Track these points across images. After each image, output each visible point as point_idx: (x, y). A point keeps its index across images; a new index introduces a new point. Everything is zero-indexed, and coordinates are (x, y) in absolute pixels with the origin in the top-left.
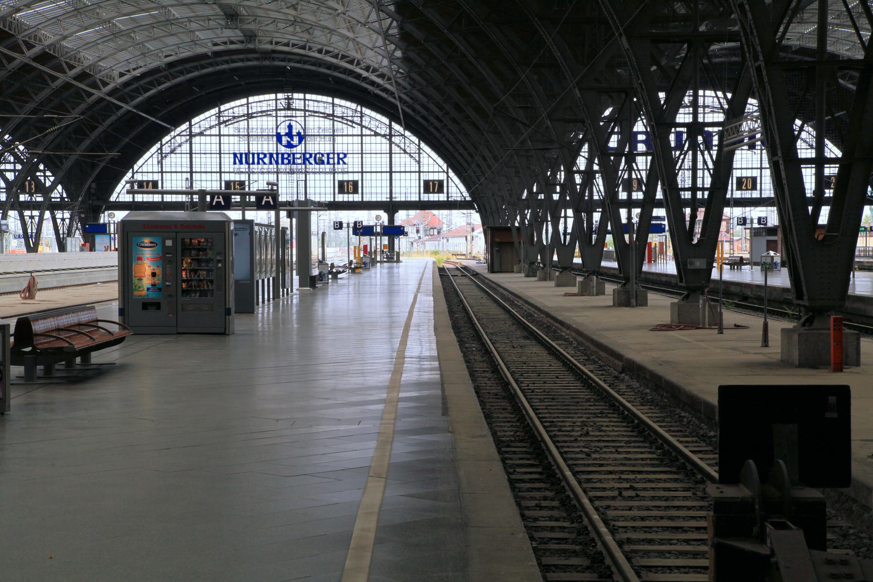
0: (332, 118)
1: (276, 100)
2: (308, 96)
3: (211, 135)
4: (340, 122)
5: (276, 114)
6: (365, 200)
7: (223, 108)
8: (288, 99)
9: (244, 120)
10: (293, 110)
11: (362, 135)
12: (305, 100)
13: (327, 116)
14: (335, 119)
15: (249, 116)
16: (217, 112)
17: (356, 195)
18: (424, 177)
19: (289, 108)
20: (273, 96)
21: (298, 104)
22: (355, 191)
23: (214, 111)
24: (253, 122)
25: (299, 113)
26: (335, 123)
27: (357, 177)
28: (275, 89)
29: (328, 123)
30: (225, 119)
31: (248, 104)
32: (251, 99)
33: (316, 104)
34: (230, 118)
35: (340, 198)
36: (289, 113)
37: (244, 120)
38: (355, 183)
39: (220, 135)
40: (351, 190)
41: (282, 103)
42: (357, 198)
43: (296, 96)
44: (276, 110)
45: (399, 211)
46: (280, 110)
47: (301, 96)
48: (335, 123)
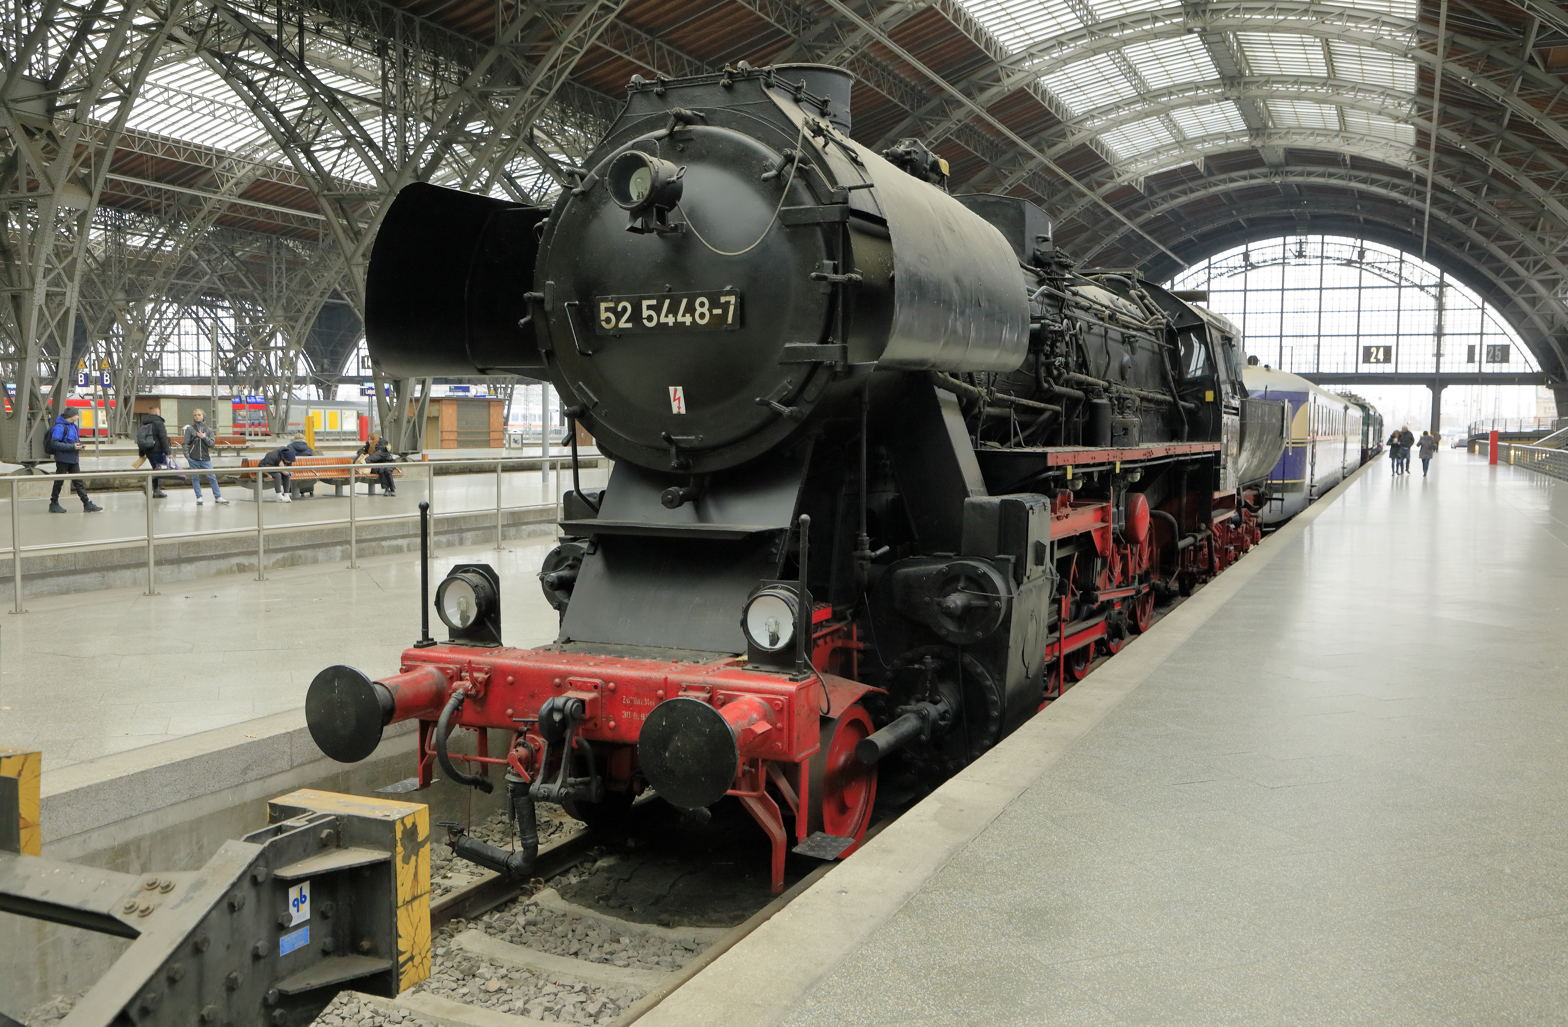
1: (1285, 244)
2: (1328, 238)
6: (1399, 371)
7: (1214, 259)
8: (1301, 243)
11: (1400, 287)
17: (1387, 365)
18: (1489, 340)
20: (1280, 240)
22: (1387, 359)
23: (1204, 263)
24: (1252, 274)
25: (1313, 261)
26: (1363, 272)
27: (1391, 341)
28: (1284, 231)
29: (1353, 272)
30: (1219, 271)
32: (1252, 246)
33: (1338, 247)
35: (1364, 369)
36: (1301, 261)
38: (1387, 350)
40: (1381, 356)
41: (1295, 248)
42: (1389, 368)
43: (1311, 238)
45: (1450, 387)
47: (1318, 238)
48: (1363, 272)
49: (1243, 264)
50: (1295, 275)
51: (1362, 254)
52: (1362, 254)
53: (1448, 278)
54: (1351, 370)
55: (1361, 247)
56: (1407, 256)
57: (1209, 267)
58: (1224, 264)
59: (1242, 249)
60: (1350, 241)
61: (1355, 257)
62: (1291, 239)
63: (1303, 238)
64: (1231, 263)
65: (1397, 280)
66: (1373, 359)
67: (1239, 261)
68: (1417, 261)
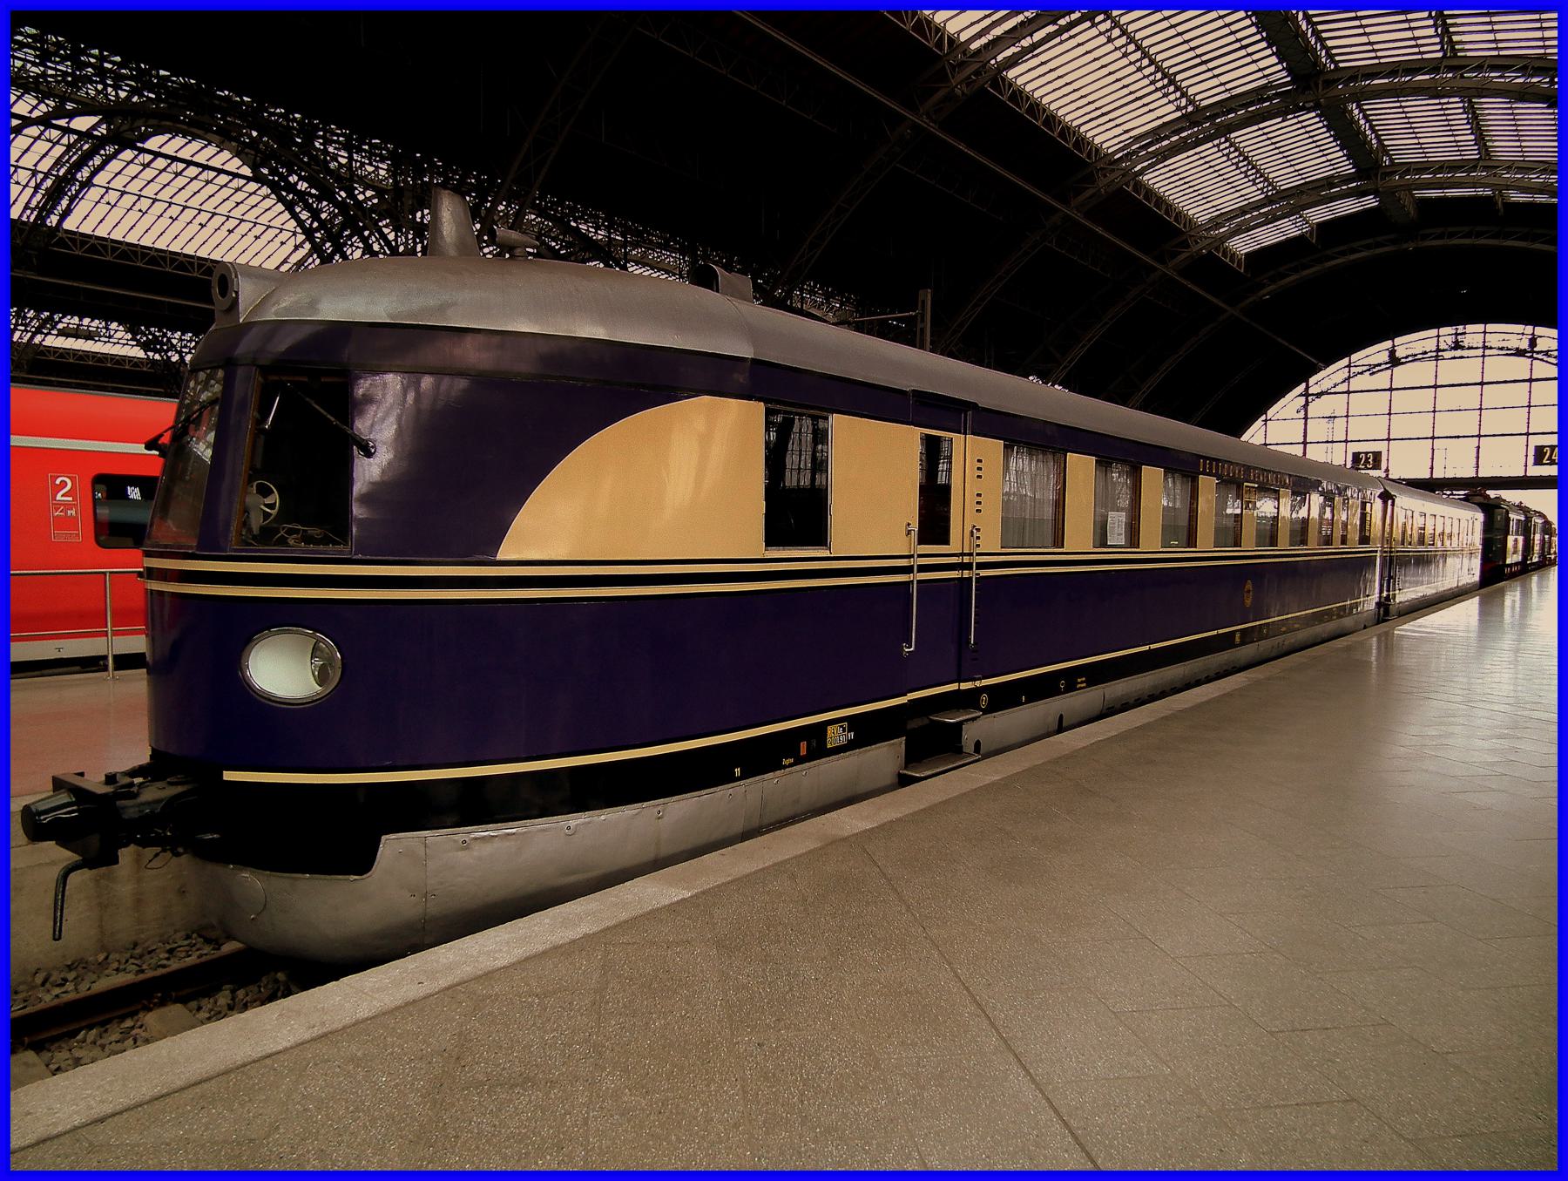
0: (1529, 355)
2: (1491, 327)
3: (1335, 393)
4: (1542, 360)
7: (1354, 357)
10: (1462, 348)
12: (1485, 332)
13: (1519, 353)
14: (1535, 355)
15: (1394, 361)
19: (1457, 346)
20: (1433, 332)
23: (1345, 361)
30: (1360, 369)
31: (1394, 346)
32: (1398, 341)
36: (1459, 353)
41: (1450, 340)
43: (1470, 328)
44: (1438, 350)
46: (1444, 350)
47: (1480, 327)
50: (1451, 370)
51: (1533, 342)
52: (1533, 342)
54: (1517, 471)
55: (1533, 334)
57: (1349, 366)
58: (1366, 362)
59: (1388, 344)
60: (1519, 328)
61: (1524, 345)
62: (1445, 330)
64: (1373, 360)
66: (1544, 461)
67: (1385, 357)
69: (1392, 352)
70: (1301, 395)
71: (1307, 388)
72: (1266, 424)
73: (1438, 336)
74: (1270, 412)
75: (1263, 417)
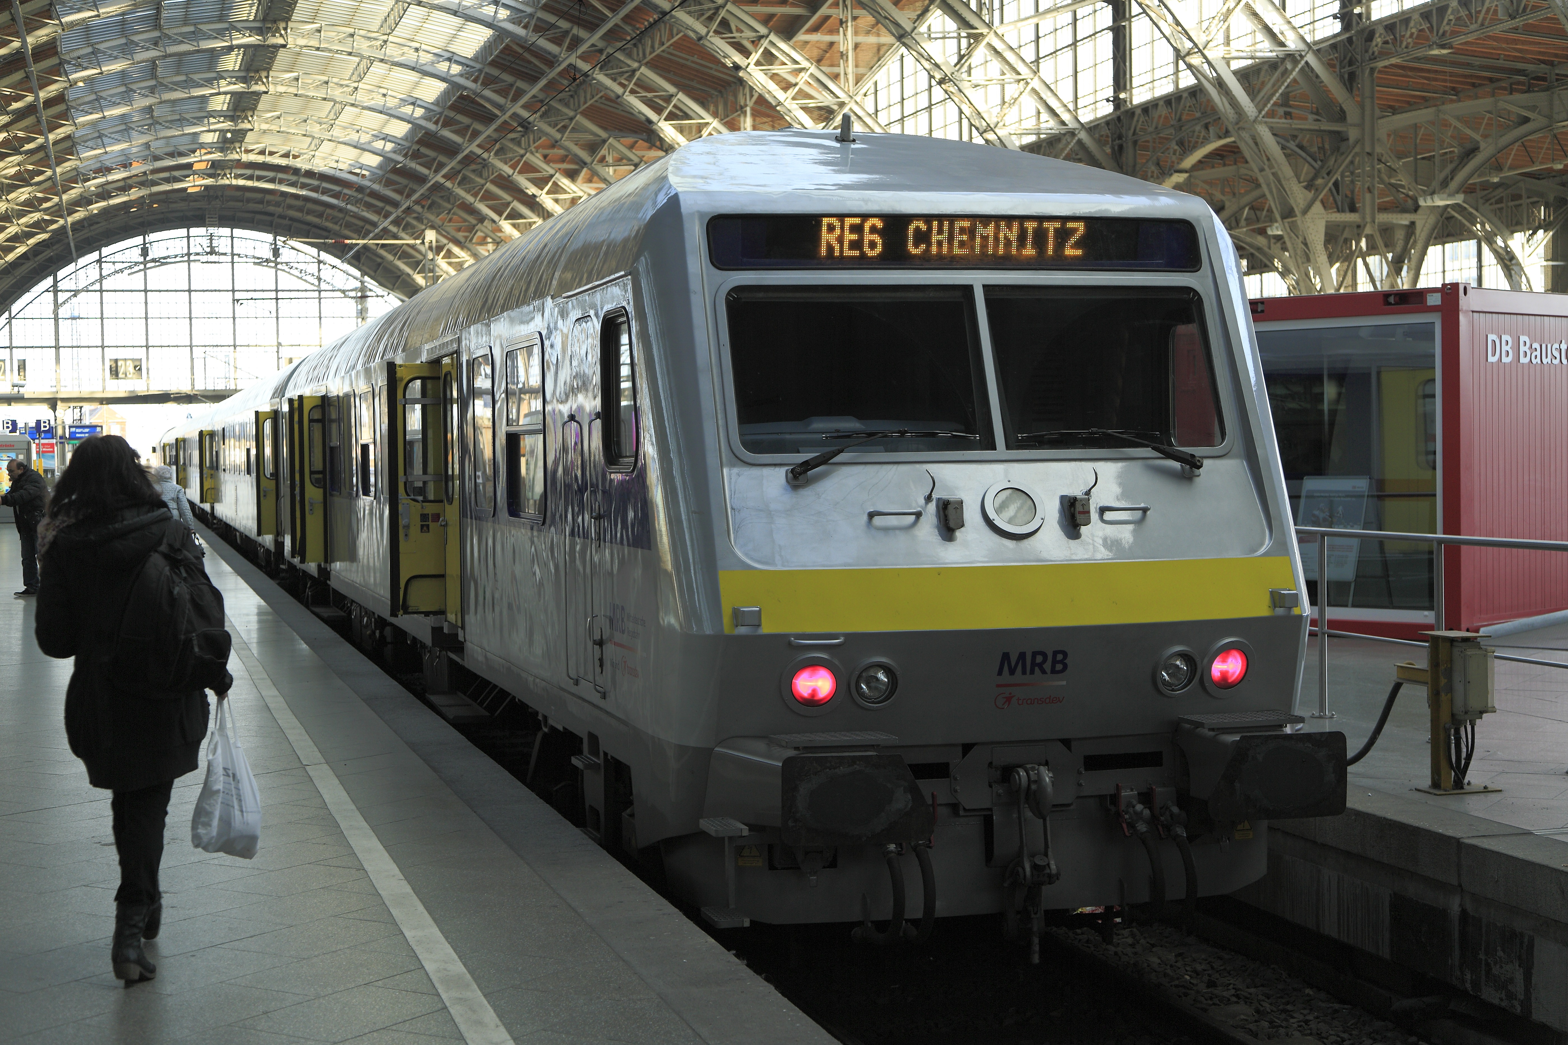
0: (273, 264)
2: (237, 232)
5: (189, 258)
7: (105, 251)
9: (140, 270)
12: (232, 237)
16: (98, 258)
20: (183, 232)
21: (223, 245)
23: (95, 255)
31: (145, 244)
34: (119, 266)
37: (140, 270)
39: (101, 291)
47: (226, 231)
49: (141, 259)
51: (276, 252)
53: (370, 283)
56: (324, 256)
57: (99, 261)
58: (118, 257)
59: (139, 240)
63: (211, 230)
65: (316, 282)
68: (336, 261)
69: (145, 252)
70: (47, 291)
71: (56, 282)
72: (9, 323)
73: (188, 237)
74: (15, 308)
75: (6, 315)
